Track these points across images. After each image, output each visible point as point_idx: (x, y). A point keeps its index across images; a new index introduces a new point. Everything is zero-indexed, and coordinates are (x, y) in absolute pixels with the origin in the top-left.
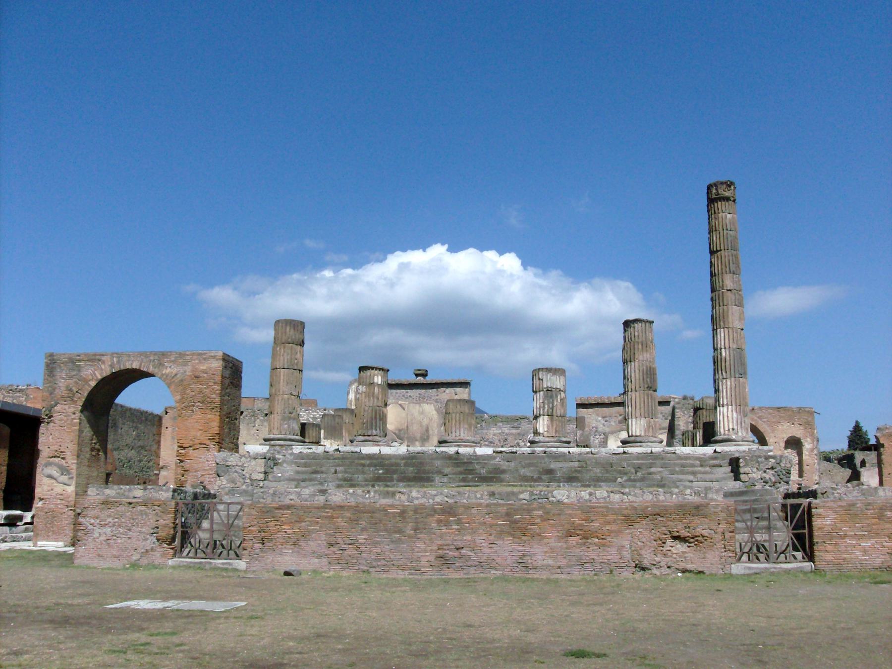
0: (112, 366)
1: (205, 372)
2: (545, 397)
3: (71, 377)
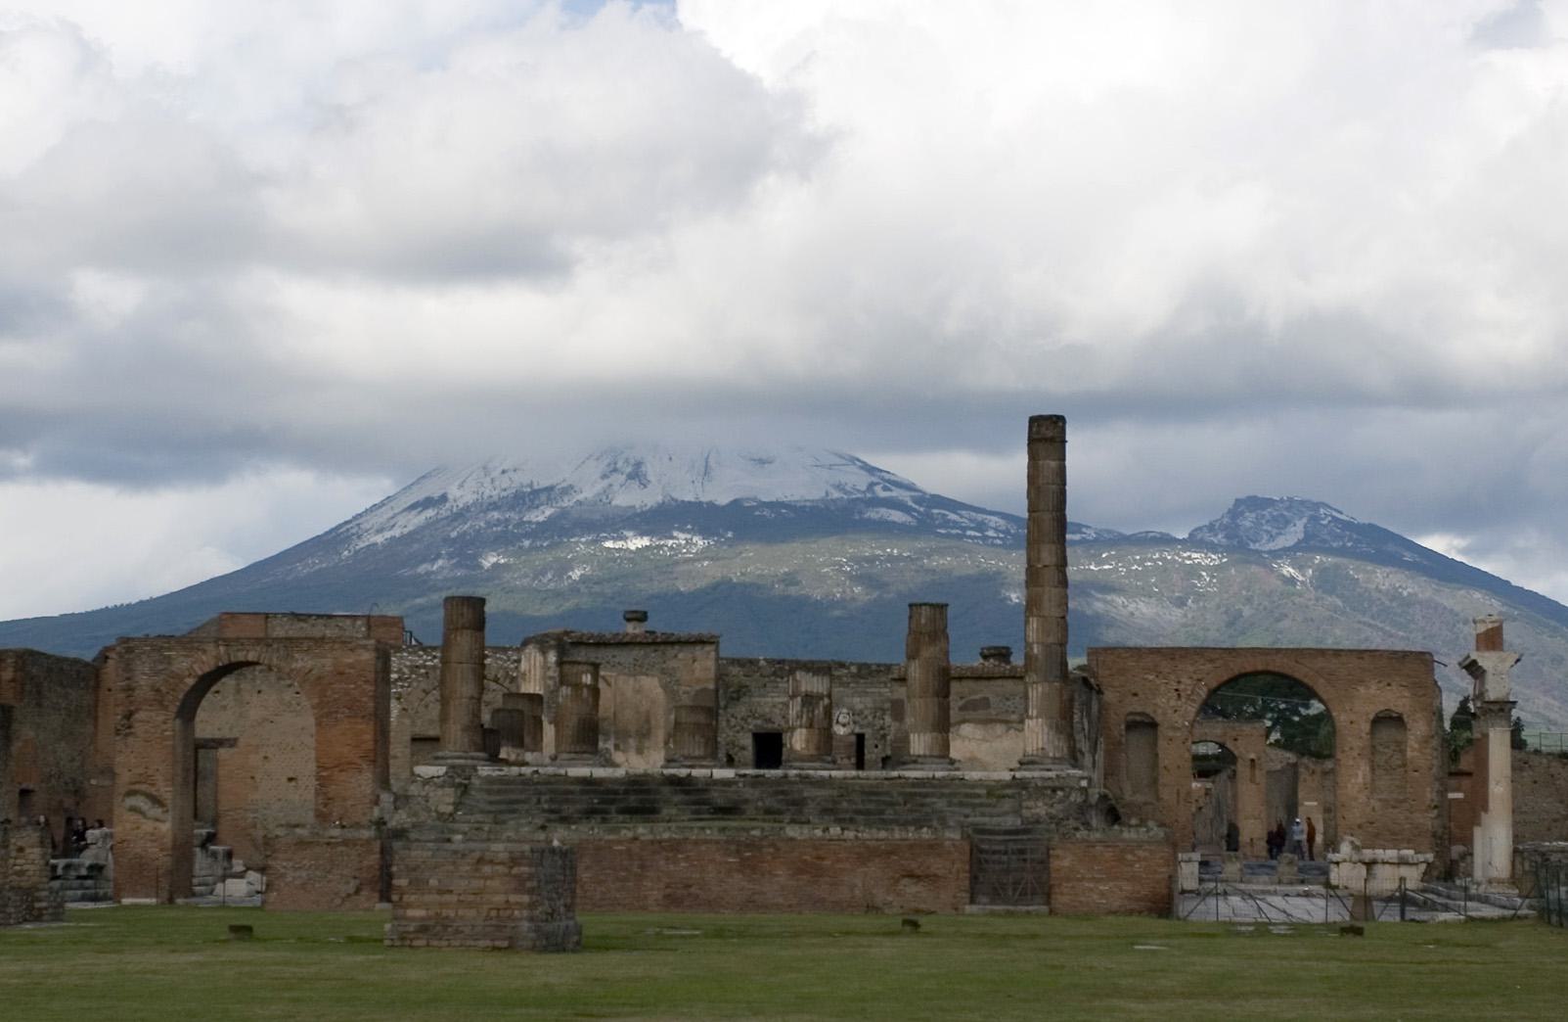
0: (218, 658)
1: (351, 666)
2: (803, 705)
3: (157, 673)
